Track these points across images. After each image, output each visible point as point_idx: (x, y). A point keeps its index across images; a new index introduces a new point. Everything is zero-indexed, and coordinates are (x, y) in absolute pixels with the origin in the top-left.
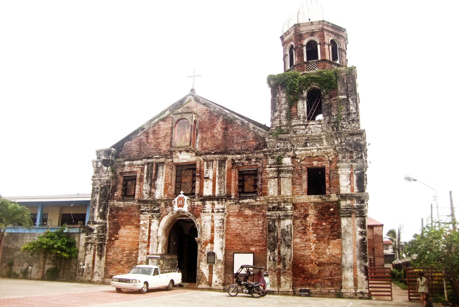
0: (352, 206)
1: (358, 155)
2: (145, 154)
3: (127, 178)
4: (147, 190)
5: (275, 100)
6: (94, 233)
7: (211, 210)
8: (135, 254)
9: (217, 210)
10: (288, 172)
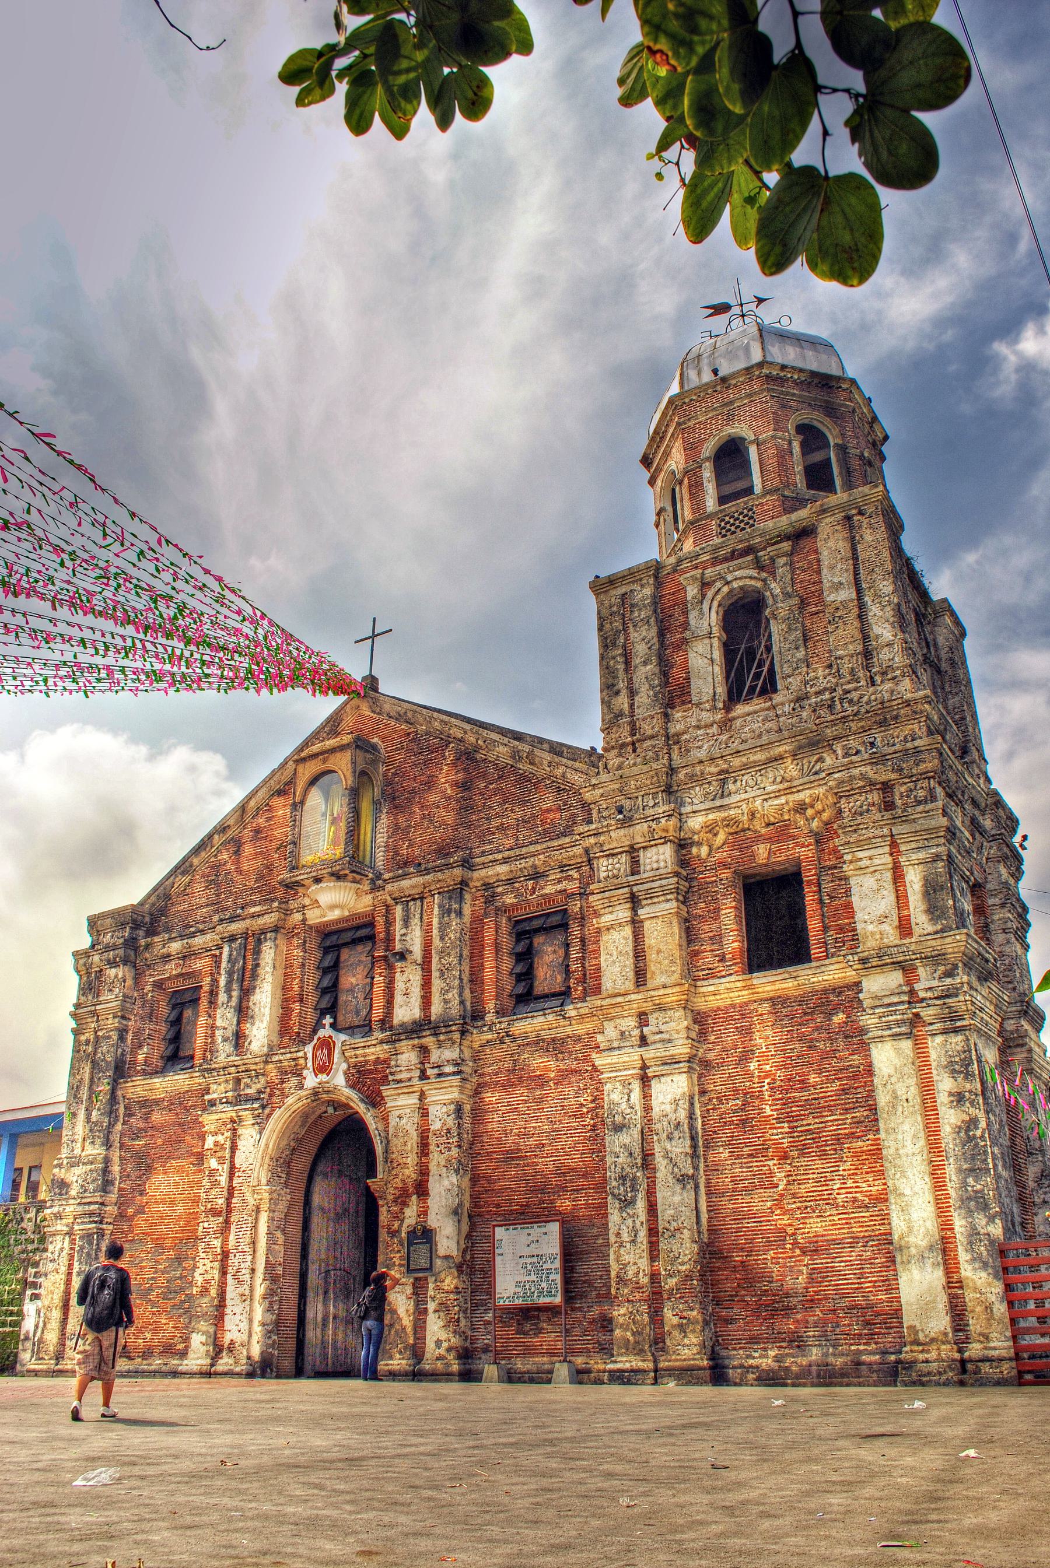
1: (914, 793)
7: (417, 1073)
9: (436, 1071)
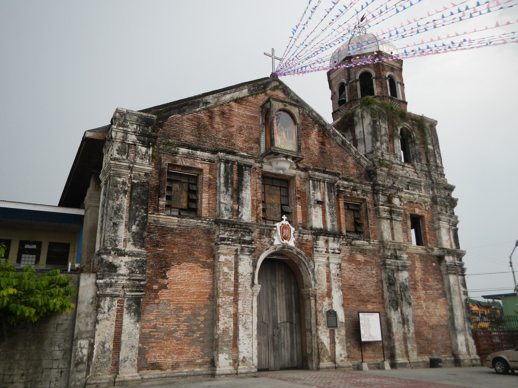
0: (455, 263)
2: (208, 145)
3: (173, 177)
4: (227, 205)
5: (376, 128)
6: (122, 275)
7: (325, 250)
8: (204, 316)
9: (332, 251)
10: (399, 214)
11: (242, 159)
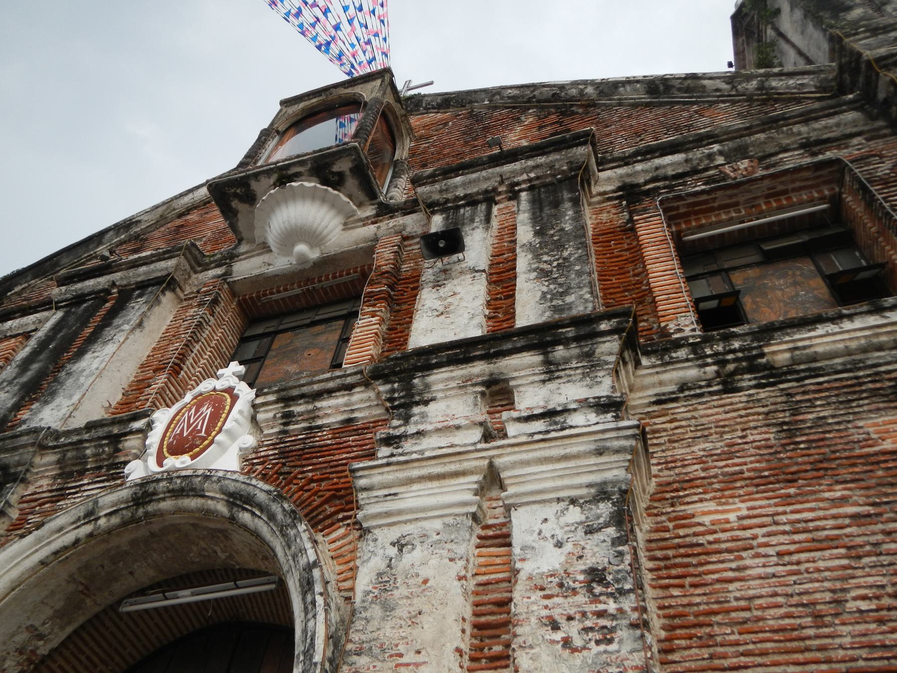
11: (131, 272)
